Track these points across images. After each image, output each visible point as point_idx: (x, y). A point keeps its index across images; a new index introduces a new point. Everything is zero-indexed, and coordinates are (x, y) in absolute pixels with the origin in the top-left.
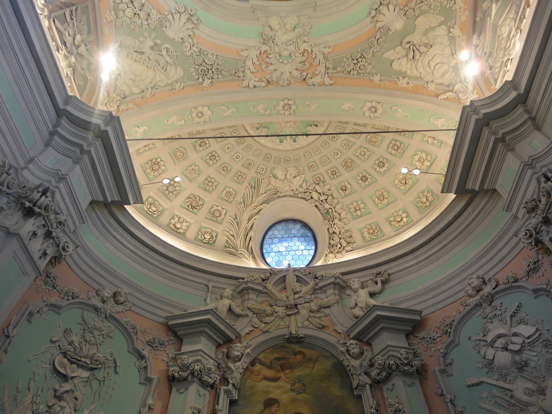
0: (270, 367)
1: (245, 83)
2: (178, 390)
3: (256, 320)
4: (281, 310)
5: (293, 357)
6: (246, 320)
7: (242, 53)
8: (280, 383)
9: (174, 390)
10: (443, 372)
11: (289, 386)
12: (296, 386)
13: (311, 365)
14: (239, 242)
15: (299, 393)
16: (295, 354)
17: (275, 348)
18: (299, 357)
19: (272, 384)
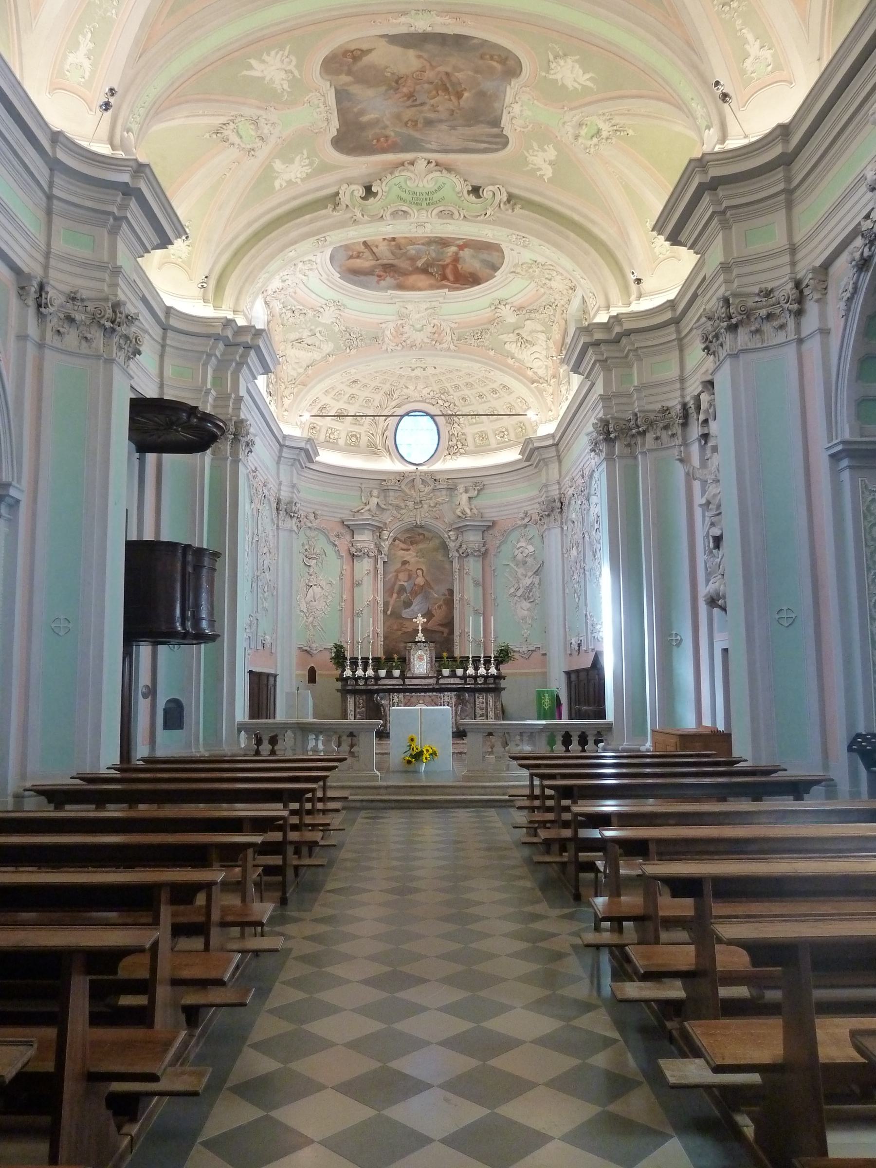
0: (404, 542)
1: (384, 347)
4: (411, 504)
6: (389, 512)
7: (381, 325)
10: (495, 555)
11: (415, 554)
14: (378, 440)
17: (407, 531)
18: (421, 537)
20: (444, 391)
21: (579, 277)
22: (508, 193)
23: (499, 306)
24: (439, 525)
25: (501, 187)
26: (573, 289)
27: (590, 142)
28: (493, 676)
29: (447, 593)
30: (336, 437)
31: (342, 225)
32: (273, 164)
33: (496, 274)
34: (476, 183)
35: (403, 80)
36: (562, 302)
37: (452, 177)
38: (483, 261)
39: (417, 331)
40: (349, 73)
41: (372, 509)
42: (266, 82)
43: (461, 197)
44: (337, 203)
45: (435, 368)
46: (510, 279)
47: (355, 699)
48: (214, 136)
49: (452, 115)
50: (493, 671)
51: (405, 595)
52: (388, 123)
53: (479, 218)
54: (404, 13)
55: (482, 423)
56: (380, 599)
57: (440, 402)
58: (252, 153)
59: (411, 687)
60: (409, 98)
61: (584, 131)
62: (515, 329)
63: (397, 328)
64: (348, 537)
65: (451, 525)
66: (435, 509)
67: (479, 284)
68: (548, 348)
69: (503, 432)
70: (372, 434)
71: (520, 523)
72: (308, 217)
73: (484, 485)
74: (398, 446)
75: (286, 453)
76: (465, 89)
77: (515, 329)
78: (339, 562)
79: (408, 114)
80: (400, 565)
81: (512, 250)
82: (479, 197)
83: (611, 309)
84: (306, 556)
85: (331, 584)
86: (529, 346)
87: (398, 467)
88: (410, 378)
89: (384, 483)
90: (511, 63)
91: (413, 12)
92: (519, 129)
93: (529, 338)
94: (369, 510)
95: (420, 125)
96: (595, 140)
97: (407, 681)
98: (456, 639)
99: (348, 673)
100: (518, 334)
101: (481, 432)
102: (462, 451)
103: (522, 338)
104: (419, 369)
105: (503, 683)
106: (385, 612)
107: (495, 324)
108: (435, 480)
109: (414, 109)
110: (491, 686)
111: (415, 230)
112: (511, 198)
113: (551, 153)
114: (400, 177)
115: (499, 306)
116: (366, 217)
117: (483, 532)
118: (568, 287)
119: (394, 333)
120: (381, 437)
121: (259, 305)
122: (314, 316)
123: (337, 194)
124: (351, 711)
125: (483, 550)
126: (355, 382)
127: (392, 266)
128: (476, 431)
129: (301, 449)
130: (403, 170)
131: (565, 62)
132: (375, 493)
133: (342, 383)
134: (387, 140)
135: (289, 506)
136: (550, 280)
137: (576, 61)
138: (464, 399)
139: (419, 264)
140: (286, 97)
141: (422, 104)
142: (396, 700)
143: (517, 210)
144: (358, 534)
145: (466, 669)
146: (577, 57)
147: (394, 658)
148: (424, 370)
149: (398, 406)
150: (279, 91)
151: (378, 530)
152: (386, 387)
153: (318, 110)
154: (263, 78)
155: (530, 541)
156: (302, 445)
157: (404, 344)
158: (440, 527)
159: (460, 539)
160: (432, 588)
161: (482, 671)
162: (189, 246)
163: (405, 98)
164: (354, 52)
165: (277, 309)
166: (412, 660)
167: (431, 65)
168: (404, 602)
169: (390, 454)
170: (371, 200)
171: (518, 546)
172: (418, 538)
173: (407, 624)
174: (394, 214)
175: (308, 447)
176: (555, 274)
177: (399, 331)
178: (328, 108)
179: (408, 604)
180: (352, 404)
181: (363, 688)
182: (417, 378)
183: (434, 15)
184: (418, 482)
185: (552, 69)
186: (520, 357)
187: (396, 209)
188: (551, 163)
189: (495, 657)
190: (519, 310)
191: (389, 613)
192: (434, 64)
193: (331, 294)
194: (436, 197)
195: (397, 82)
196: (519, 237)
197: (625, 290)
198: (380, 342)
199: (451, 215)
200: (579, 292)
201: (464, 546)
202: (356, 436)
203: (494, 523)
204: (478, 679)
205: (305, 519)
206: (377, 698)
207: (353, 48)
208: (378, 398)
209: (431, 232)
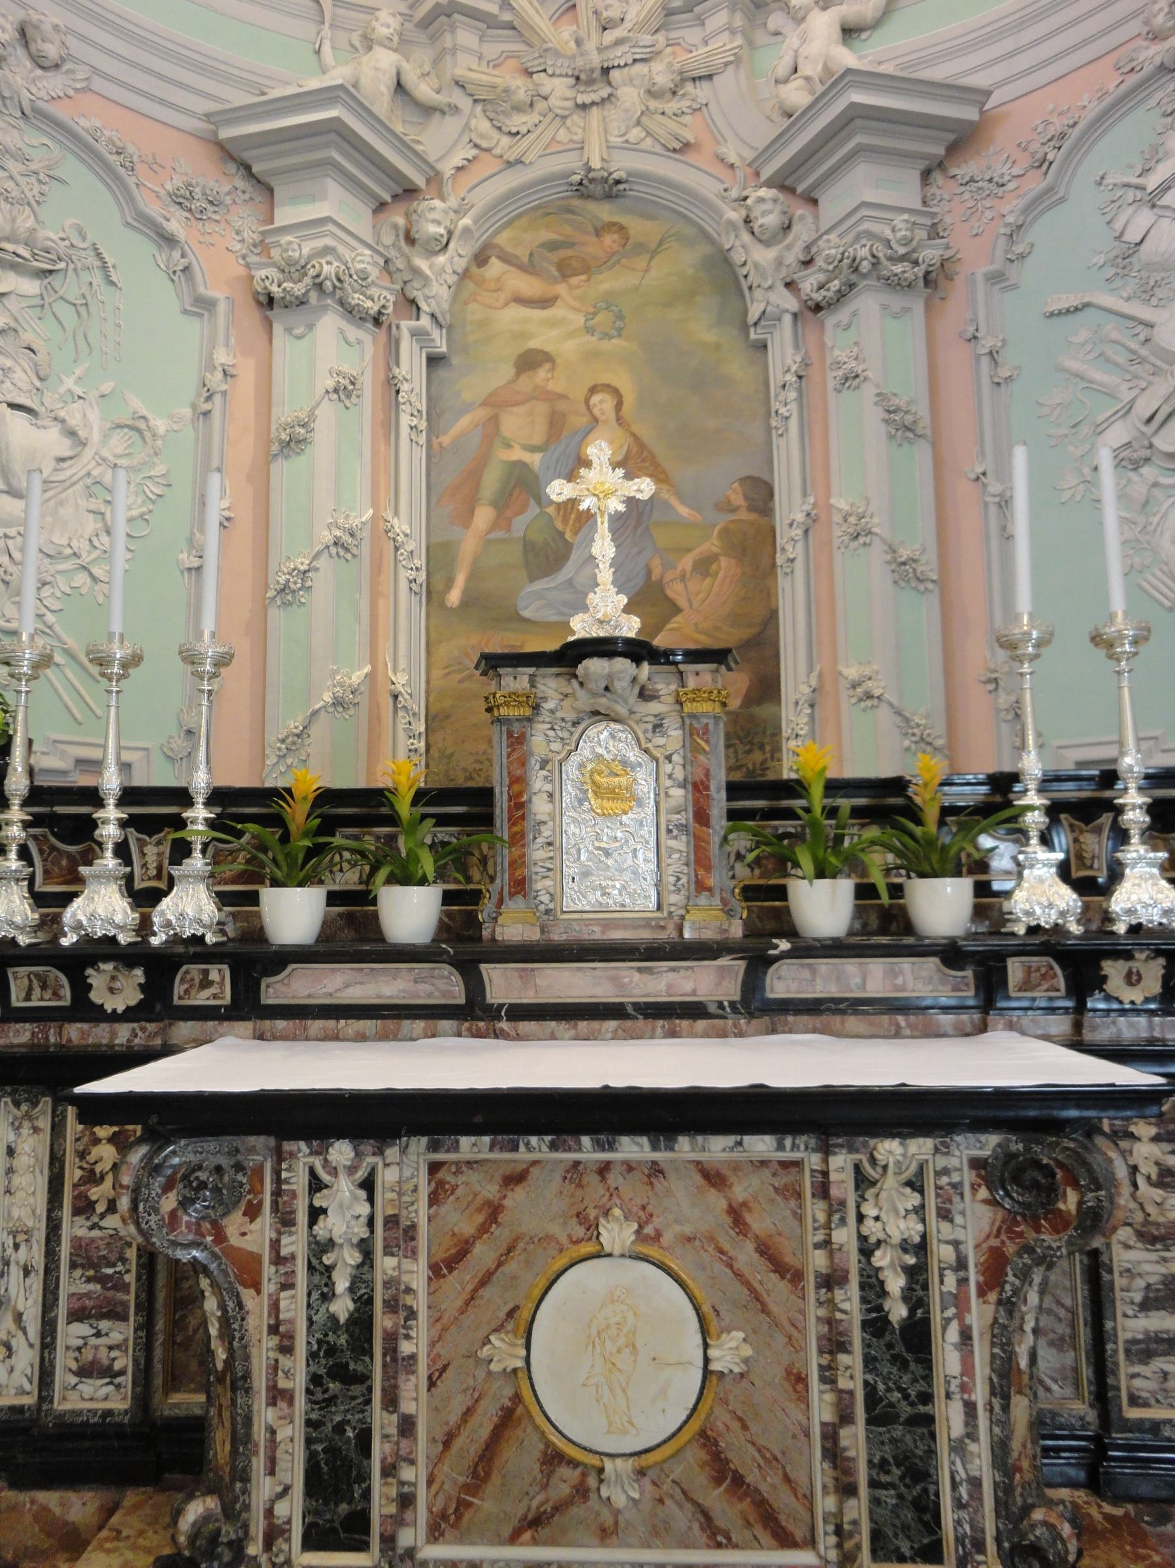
8: (556, 312)
12: (599, 318)
13: (641, 262)
19: (537, 314)
29: (738, 499)
51: (533, 509)
80: (507, 371)
85: (137, 427)
117: (926, 175)
144: (295, 199)
166: (540, 807)
168: (528, 547)
172: (593, 248)
191: (454, 597)
204: (1113, 970)
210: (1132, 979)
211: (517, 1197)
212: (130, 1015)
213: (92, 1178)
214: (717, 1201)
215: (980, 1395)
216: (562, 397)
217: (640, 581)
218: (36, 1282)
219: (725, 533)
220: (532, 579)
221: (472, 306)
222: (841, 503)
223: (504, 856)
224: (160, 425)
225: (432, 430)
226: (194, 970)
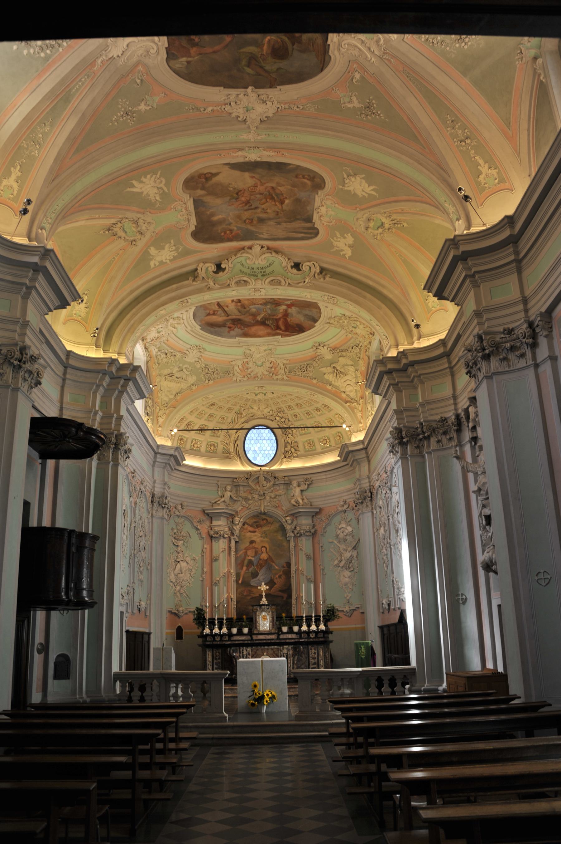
0: (251, 526)
1: (234, 379)
2: (215, 541)
3: (244, 503)
4: (256, 496)
5: (262, 521)
6: (239, 503)
7: (232, 363)
8: (256, 534)
9: (213, 541)
10: (321, 535)
11: (260, 535)
14: (231, 448)
15: (264, 538)
16: (263, 520)
17: (254, 517)
18: (265, 521)
19: (253, 534)
20: (280, 411)
21: (375, 324)
22: (320, 267)
23: (319, 347)
24: (278, 512)
25: (315, 263)
26: (373, 334)
27: (376, 232)
28: (322, 631)
29: (285, 566)
30: (199, 446)
31: (199, 291)
32: (149, 250)
33: (315, 325)
34: (297, 260)
35: (242, 192)
36: (365, 344)
37: (279, 257)
38: (306, 316)
39: (258, 366)
40: (203, 188)
41: (226, 500)
42: (144, 195)
43: (286, 270)
44: (196, 275)
45: (273, 393)
46: (326, 328)
47: (213, 652)
48: (107, 232)
49: (278, 215)
50: (322, 627)
51: (253, 567)
52: (232, 221)
53: (300, 285)
54: (241, 149)
55: (310, 433)
56: (233, 571)
57: (278, 418)
58: (134, 243)
59: (257, 642)
60: (246, 204)
61: (372, 224)
62: (331, 363)
63: (243, 365)
64: (208, 523)
65: (288, 512)
66: (275, 500)
67: (304, 332)
68: (356, 377)
69: (325, 440)
70: (227, 443)
71: (340, 509)
72: (174, 286)
73: (312, 481)
74: (247, 452)
75: (159, 459)
76: (286, 198)
77: (331, 363)
78: (200, 542)
79: (246, 215)
80: (248, 544)
81: (326, 307)
82: (299, 270)
83: (399, 347)
84: (175, 538)
85: (194, 559)
86: (342, 376)
87: (249, 468)
88: (254, 401)
89: (235, 480)
90: (317, 180)
91: (247, 149)
92: (325, 224)
93: (342, 370)
94: (224, 501)
95: (255, 222)
96: (380, 230)
97: (254, 637)
98: (294, 602)
99: (207, 631)
100: (334, 367)
101: (309, 440)
102: (295, 455)
103: (337, 370)
104: (261, 394)
105: (331, 637)
106: (237, 581)
107: (316, 361)
108: (275, 477)
109: (250, 211)
110: (321, 639)
111: (253, 293)
112: (323, 271)
113: (350, 240)
114: (242, 258)
115: (319, 347)
116: (217, 285)
117: (313, 517)
118: (368, 333)
119: (241, 368)
120: (233, 445)
121: (139, 349)
122: (182, 357)
123: (196, 270)
124: (210, 662)
125: (313, 531)
126: (213, 404)
127: (239, 320)
128: (305, 440)
129: (171, 455)
130: (244, 253)
131: (356, 179)
132: (229, 488)
133: (203, 405)
134: (231, 233)
135: (161, 499)
136: (355, 328)
137: (363, 178)
138: (296, 416)
139: (259, 318)
140: (158, 205)
141: (256, 208)
142: (245, 652)
143: (328, 278)
144: (216, 520)
145: (300, 626)
146: (364, 176)
147: (243, 619)
148: (265, 395)
149: (246, 422)
150: (153, 201)
151: (231, 517)
152: (237, 408)
153: (181, 213)
154: (142, 193)
155: (348, 523)
156: (172, 452)
157: (249, 376)
158: (279, 513)
159: (295, 523)
160: (274, 562)
161: (313, 628)
162: (86, 308)
163: (244, 204)
164: (207, 175)
165: (154, 353)
166: (258, 620)
167: (261, 182)
168: (252, 573)
169: (240, 458)
170: (221, 273)
171: (340, 527)
172: (262, 523)
173: (254, 590)
174: (238, 283)
175: (177, 454)
176: (358, 323)
177: (245, 367)
178: (188, 212)
179: (255, 575)
180: (211, 421)
181: (219, 643)
182: (260, 401)
183: (262, 151)
184: (262, 479)
185: (346, 184)
186: (336, 384)
187: (239, 279)
188: (350, 246)
189: (323, 616)
190: (334, 350)
191: (240, 582)
192: (263, 181)
193: (194, 341)
194: (268, 270)
195: (237, 194)
196: (329, 297)
197: (409, 334)
198: (231, 375)
199: (279, 283)
200: (377, 337)
201: (298, 528)
202: (214, 445)
203: (321, 509)
204: (311, 635)
205: (174, 509)
206: (230, 651)
207: (205, 172)
208: (231, 416)
209: (265, 295)
210: (312, 635)
211: (258, 651)
212: (219, 641)
213: (216, 656)
214: (272, 651)
215: (291, 664)
216: (257, 548)
217: (270, 579)
218: (211, 666)
219: (283, 571)
220: (253, 578)
221: (242, 533)
222: (300, 569)
223: (254, 625)
224: (197, 558)
225: (236, 554)
226: (224, 637)
